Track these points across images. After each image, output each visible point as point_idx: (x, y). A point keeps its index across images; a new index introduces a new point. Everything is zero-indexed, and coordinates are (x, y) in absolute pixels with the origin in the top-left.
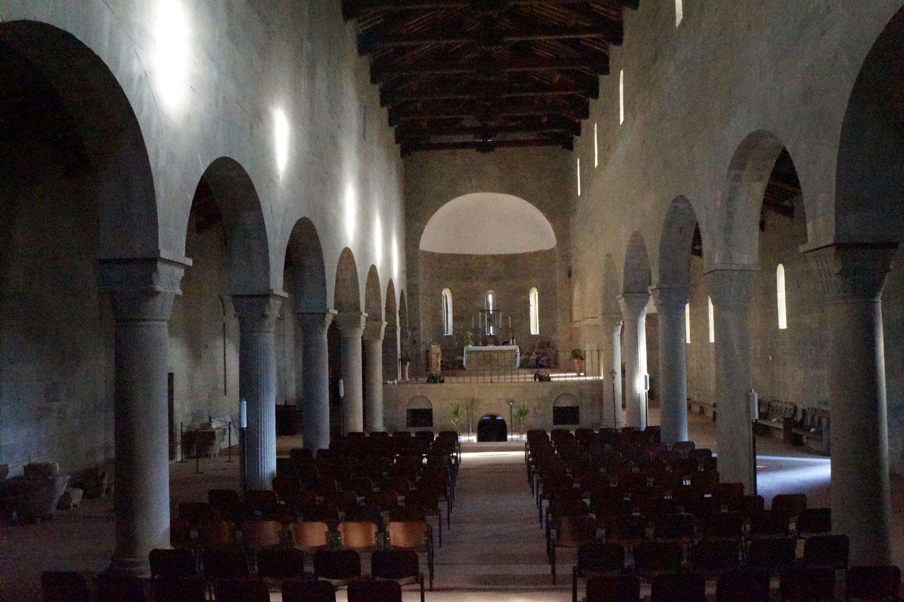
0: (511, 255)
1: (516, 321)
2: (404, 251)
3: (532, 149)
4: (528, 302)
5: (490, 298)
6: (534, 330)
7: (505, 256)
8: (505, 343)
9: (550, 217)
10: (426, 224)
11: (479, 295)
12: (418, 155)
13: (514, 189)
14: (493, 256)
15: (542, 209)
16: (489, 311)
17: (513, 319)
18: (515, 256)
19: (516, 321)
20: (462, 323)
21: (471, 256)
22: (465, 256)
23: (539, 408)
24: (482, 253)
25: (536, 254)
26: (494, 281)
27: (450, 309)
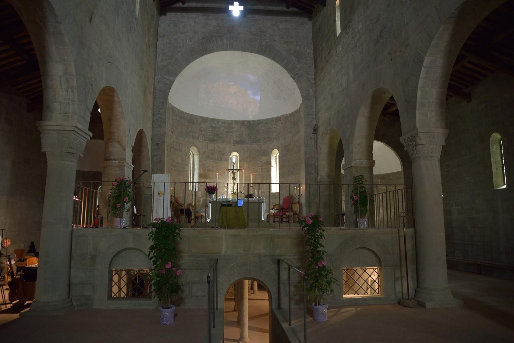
3: (281, 18)
6: (275, 189)
7: (249, 122)
9: (296, 76)
10: (176, 75)
11: (224, 157)
12: (171, 17)
14: (237, 122)
15: (289, 71)
18: (258, 123)
21: (218, 121)
22: (213, 120)
24: (229, 119)
25: (278, 119)
26: (238, 144)
27: (196, 167)
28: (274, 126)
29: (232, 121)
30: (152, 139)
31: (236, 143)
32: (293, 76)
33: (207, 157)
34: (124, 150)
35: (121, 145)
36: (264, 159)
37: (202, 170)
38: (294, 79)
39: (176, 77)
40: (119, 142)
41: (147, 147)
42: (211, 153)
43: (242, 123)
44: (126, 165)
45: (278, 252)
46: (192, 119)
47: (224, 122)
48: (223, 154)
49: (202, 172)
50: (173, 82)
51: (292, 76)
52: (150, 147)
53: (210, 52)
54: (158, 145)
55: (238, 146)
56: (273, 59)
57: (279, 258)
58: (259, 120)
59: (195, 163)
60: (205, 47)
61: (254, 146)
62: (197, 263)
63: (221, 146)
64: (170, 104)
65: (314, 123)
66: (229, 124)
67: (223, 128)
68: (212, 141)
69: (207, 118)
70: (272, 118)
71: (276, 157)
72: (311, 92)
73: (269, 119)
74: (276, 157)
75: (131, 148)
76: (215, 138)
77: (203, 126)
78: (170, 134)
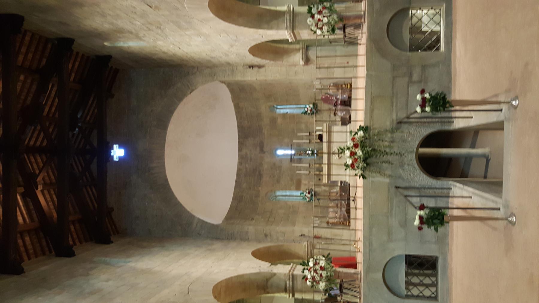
0: (239, 132)
1: (303, 126)
2: (218, 245)
4: (284, 115)
5: (280, 152)
8: (321, 137)
10: (193, 217)
13: (163, 123)
14: (240, 150)
16: (291, 155)
17: (301, 131)
19: (303, 126)
20: (304, 182)
21: (239, 170)
23: (411, 75)
27: (288, 193)
28: (244, 110)
29: (239, 155)
30: (259, 242)
31: (262, 151)
32: (190, 91)
33: (278, 181)
34: (275, 274)
35: (270, 278)
36: (279, 121)
37: (292, 187)
38: (193, 90)
39: (194, 216)
40: (267, 280)
41: (269, 248)
42: (273, 177)
43: (241, 144)
44: (291, 272)
45: (388, 123)
46: (237, 199)
47: (240, 163)
48: (274, 164)
49: (294, 187)
50: (199, 219)
51: (190, 93)
52: (269, 245)
53: (167, 180)
54: (266, 236)
55: (265, 149)
56: (171, 112)
57: (395, 122)
58: (238, 126)
59: (284, 194)
60: (163, 188)
61: (265, 131)
62: (399, 207)
63: (266, 166)
64: (223, 221)
65: (240, 68)
66: (242, 159)
67: (247, 165)
68: (260, 175)
69: (236, 181)
70: (236, 113)
71: (277, 108)
72: (207, 71)
73: (236, 116)
74: (277, 108)
75: (272, 266)
76: (257, 173)
77: (244, 185)
78: (254, 221)
